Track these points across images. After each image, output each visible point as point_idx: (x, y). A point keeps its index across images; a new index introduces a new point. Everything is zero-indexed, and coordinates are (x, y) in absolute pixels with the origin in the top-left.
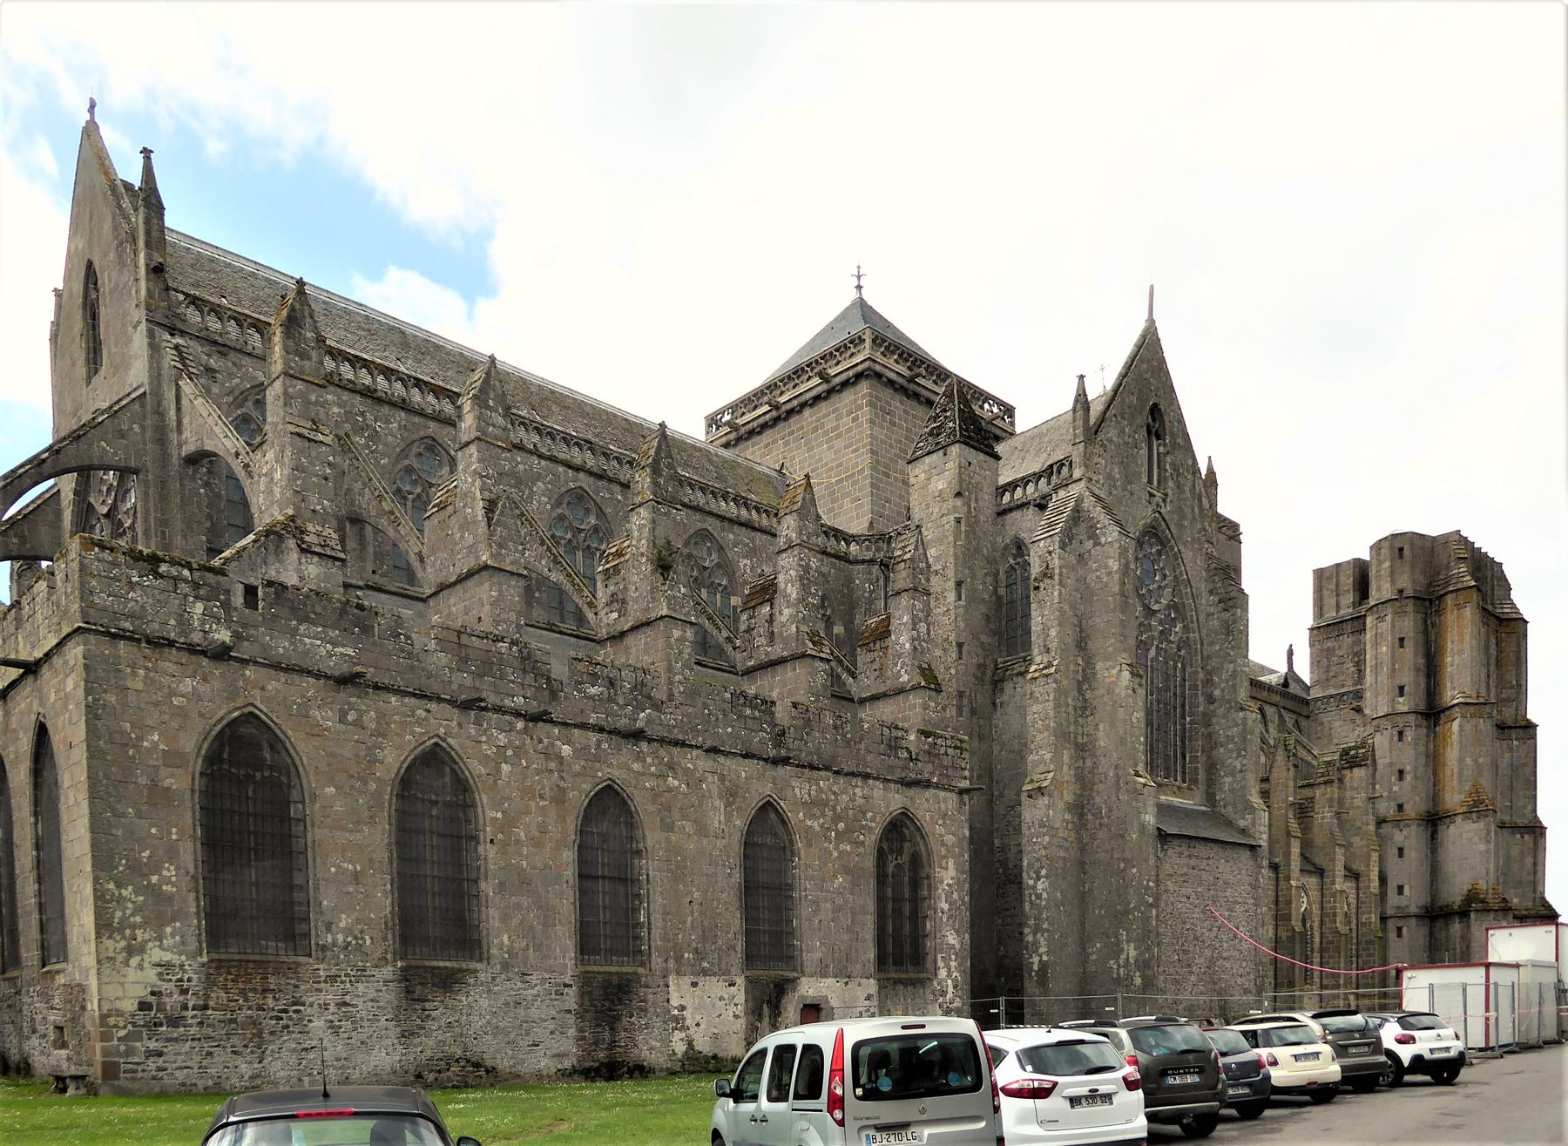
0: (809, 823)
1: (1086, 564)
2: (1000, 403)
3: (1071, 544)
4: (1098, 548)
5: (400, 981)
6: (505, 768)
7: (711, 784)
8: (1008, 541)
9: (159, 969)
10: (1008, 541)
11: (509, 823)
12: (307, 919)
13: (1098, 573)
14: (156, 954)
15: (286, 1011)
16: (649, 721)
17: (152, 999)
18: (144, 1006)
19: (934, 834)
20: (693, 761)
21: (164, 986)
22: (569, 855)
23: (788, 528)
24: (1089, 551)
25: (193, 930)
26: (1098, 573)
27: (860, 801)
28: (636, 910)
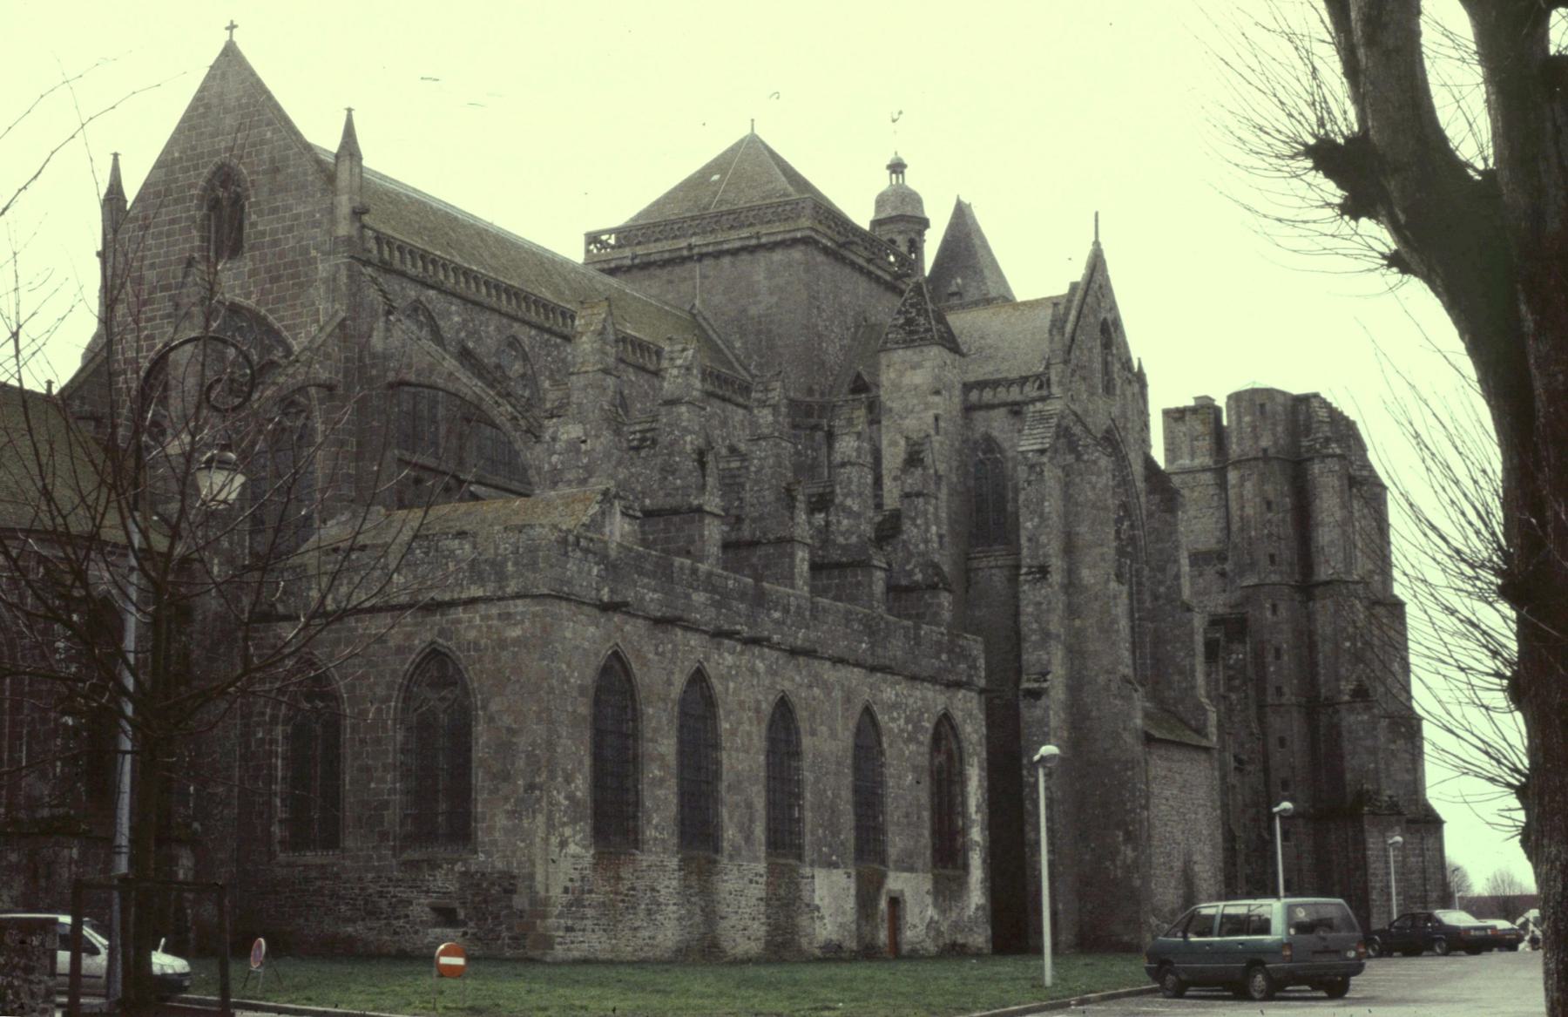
0: (891, 725)
5: (680, 869)
6: (732, 685)
7: (837, 694)
9: (572, 860)
11: (733, 732)
12: (635, 817)
14: (573, 848)
15: (626, 895)
16: (804, 640)
17: (569, 884)
18: (566, 890)
20: (829, 673)
21: (576, 875)
22: (762, 758)
25: (588, 829)
28: (791, 807)
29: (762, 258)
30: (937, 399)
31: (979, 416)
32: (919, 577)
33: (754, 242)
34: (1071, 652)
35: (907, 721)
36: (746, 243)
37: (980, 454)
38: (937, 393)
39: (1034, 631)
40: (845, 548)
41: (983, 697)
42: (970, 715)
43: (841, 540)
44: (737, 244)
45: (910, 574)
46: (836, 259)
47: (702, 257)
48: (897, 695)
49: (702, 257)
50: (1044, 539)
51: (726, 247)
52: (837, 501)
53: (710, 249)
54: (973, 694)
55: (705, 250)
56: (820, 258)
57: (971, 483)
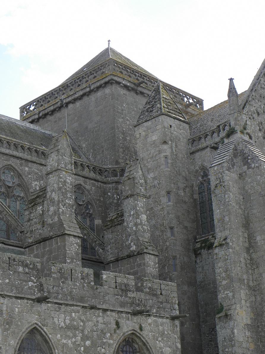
1: (244, 179)
2: (193, 97)
3: (233, 168)
4: (250, 170)
8: (197, 168)
10: (197, 168)
13: (252, 184)
19: (156, 348)
23: (53, 160)
24: (245, 172)
26: (252, 184)
27: (101, 326)
29: (93, 97)
30: (165, 147)
31: (197, 155)
32: (134, 248)
33: (88, 89)
34: (254, 290)
35: (85, 338)
36: (84, 91)
37: (200, 178)
38: (165, 142)
39: (224, 279)
40: (52, 226)
41: (177, 322)
42: (162, 334)
43: (50, 221)
44: (81, 93)
45: (129, 246)
46: (137, 93)
47: (67, 104)
48: (72, 320)
49: (67, 104)
50: (227, 219)
51: (76, 96)
52: (48, 196)
53: (70, 99)
54: (164, 320)
55: (68, 100)
56: (123, 92)
57: (196, 196)
